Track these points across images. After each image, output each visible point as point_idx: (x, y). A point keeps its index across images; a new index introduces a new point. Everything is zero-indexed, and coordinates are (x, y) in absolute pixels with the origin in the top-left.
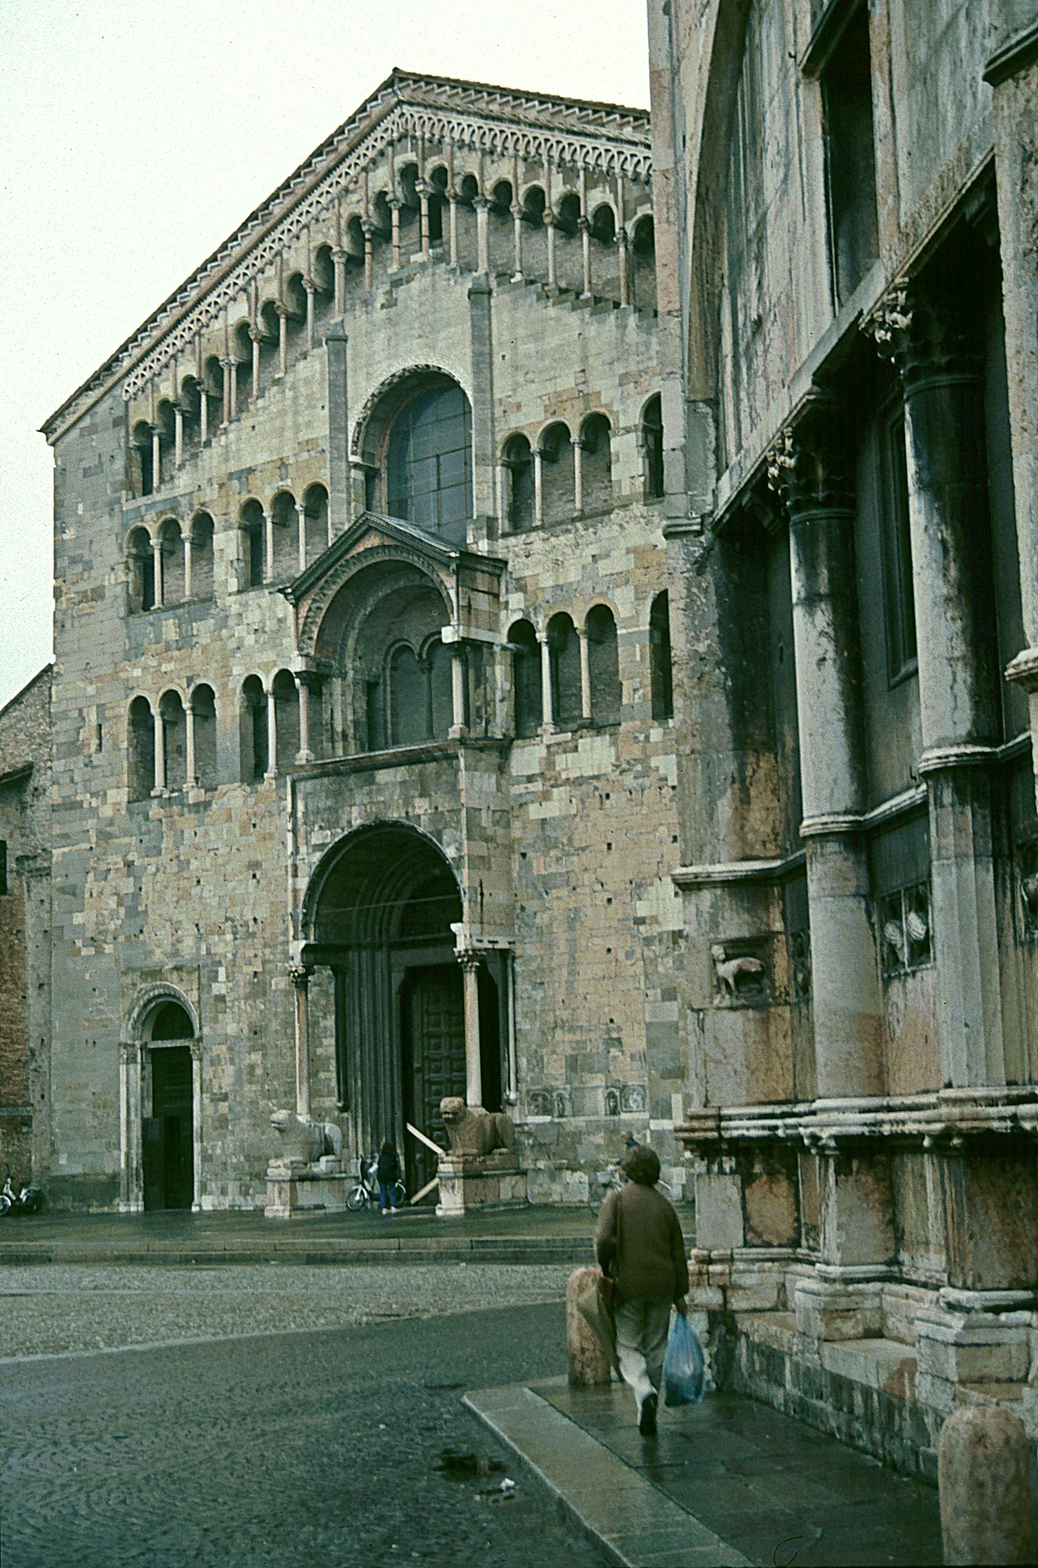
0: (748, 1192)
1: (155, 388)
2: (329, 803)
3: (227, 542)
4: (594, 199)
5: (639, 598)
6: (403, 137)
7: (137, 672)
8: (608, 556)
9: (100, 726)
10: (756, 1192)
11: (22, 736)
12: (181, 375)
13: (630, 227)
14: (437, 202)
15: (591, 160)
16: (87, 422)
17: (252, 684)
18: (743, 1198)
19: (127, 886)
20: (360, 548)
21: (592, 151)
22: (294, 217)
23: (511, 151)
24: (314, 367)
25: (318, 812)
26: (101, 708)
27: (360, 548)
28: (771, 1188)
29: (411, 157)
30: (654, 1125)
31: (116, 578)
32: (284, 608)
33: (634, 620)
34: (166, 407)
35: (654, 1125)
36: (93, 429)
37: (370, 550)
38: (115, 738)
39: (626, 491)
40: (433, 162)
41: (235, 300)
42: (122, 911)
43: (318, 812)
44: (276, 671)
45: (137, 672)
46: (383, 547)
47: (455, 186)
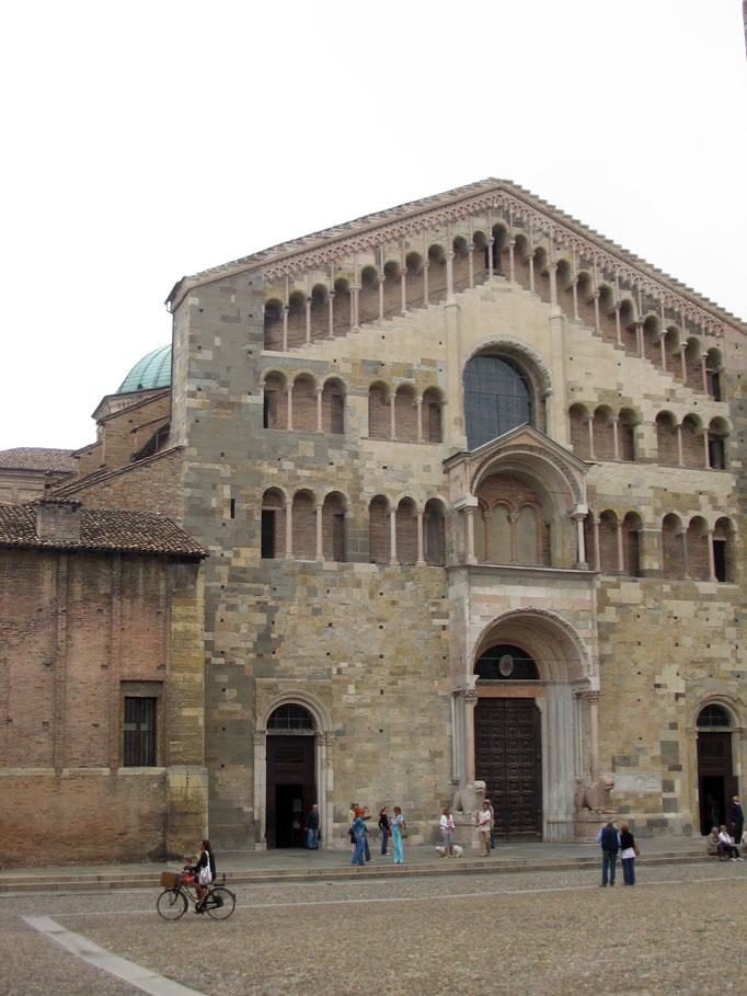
1: (291, 282)
4: (619, 295)
5: (657, 513)
6: (500, 207)
7: (274, 471)
8: (637, 487)
9: (233, 501)
12: (316, 282)
13: (645, 317)
15: (625, 275)
16: (227, 284)
19: (261, 619)
21: (622, 271)
22: (419, 219)
24: (429, 315)
26: (234, 488)
29: (502, 221)
30: (666, 795)
33: (652, 525)
34: (296, 301)
35: (666, 795)
36: (234, 291)
38: (250, 514)
39: (647, 456)
40: (517, 231)
42: (254, 636)
44: (401, 496)
45: (274, 471)
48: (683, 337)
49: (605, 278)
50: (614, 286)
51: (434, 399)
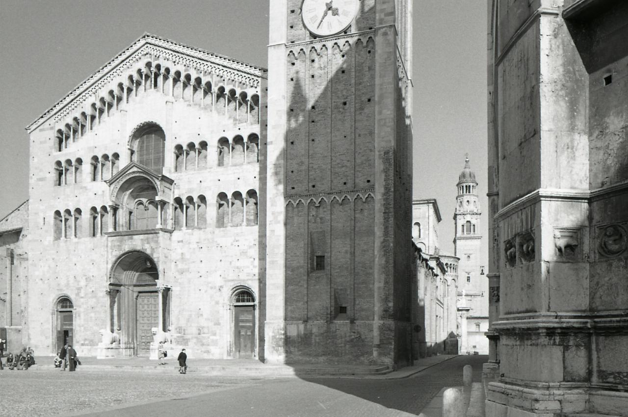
0: (566, 354)
2: (118, 244)
3: (87, 167)
10: (570, 354)
11: (18, 219)
14: (157, 76)
17: (94, 209)
18: (564, 357)
20: (131, 171)
23: (181, 62)
25: (115, 246)
27: (131, 171)
28: (577, 353)
31: (54, 175)
32: (106, 186)
37: (134, 172)
41: (91, 96)
43: (115, 246)
46: (138, 172)
47: (163, 71)
48: (238, 92)
49: (197, 73)
50: (201, 76)
51: (116, 156)
